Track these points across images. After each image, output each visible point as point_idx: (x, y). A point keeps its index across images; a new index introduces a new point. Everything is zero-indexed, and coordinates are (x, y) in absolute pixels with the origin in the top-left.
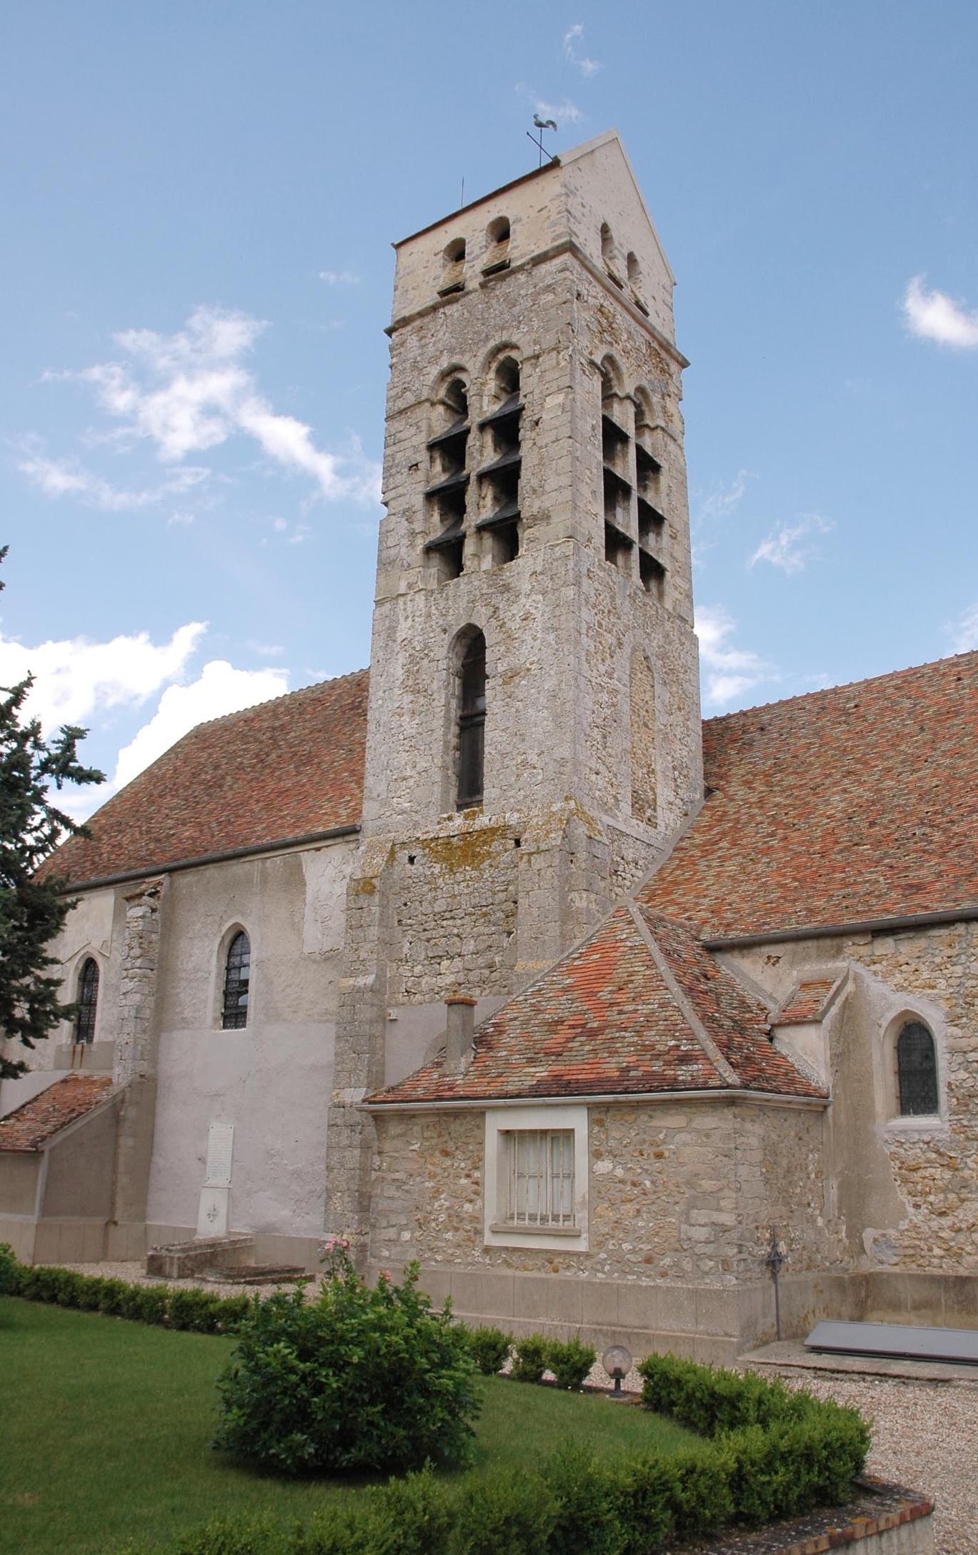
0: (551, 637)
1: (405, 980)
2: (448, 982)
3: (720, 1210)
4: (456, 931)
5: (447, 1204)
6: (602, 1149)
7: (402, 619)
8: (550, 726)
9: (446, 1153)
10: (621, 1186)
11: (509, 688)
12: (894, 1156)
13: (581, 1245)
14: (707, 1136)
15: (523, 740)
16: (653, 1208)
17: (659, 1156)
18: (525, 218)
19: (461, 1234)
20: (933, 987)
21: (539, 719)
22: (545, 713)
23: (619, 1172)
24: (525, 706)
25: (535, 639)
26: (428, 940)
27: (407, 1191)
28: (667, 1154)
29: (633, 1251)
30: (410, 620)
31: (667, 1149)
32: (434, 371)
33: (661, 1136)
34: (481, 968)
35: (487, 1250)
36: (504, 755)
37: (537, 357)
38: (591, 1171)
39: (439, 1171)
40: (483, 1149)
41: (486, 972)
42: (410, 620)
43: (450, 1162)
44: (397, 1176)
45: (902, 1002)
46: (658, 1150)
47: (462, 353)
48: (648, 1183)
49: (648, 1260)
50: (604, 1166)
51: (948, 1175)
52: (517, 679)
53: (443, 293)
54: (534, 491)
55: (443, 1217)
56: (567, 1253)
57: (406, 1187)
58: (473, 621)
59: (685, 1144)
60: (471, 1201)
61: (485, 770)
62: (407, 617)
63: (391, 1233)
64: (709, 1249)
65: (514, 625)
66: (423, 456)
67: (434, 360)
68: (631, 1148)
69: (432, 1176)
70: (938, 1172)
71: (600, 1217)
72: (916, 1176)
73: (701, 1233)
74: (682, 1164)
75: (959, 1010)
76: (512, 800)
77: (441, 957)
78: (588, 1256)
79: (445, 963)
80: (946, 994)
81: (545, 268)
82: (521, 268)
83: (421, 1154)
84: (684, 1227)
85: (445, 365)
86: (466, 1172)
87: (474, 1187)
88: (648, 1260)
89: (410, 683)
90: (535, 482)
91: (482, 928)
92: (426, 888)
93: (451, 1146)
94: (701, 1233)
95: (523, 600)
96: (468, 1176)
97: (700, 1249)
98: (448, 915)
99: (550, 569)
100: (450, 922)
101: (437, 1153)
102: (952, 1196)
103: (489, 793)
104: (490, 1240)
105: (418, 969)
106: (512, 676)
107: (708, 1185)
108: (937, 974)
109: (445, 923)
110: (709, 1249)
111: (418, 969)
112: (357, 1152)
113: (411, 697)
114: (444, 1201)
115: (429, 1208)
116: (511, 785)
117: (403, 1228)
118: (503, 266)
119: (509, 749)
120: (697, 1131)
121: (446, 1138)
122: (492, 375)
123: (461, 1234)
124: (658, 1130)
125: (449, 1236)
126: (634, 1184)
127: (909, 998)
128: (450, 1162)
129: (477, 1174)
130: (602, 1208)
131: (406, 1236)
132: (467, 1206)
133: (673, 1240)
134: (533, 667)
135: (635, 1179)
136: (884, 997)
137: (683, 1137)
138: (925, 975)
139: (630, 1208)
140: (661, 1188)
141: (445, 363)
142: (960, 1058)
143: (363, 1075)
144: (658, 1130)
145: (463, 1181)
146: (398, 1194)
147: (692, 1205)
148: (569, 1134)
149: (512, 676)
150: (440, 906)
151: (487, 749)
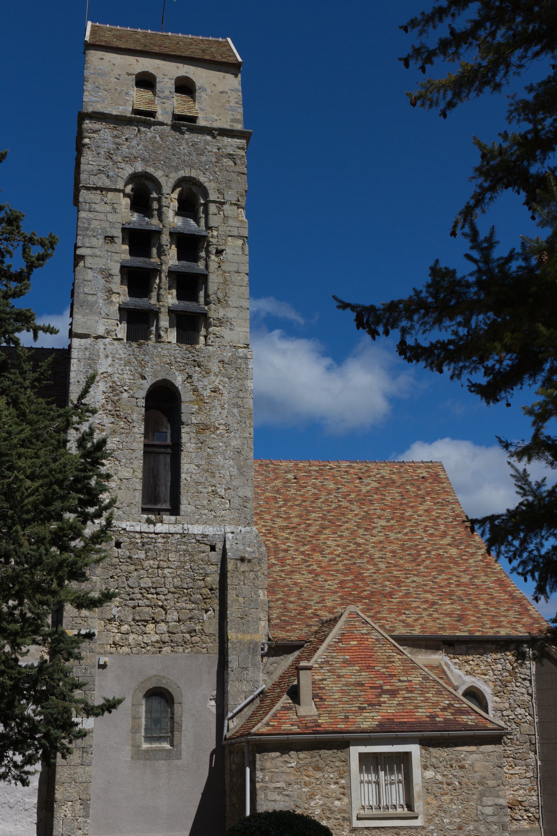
0: (235, 411)
1: (112, 634)
2: (154, 639)
3: (498, 797)
4: (160, 603)
5: (321, 802)
6: (428, 764)
7: (102, 356)
8: (235, 472)
9: (317, 768)
10: (441, 785)
11: (200, 436)
13: (418, 823)
14: (489, 756)
15: (214, 477)
16: (460, 797)
17: (462, 767)
18: (209, 91)
20: (486, 675)
21: (227, 466)
22: (231, 462)
23: (439, 777)
24: (215, 454)
25: (223, 408)
26: (134, 608)
27: (287, 795)
28: (467, 766)
29: (450, 823)
30: (110, 359)
31: (467, 763)
32: (129, 170)
33: (462, 756)
34: (182, 633)
35: (354, 830)
36: (198, 483)
37: (223, 204)
38: (423, 778)
39: (312, 780)
40: (348, 765)
41: (187, 636)
42: (110, 359)
43: (322, 774)
44: (278, 785)
45: (470, 681)
46: (460, 764)
47: (157, 168)
48: (457, 783)
49: (460, 828)
50: (430, 774)
52: (208, 432)
53: (136, 112)
54: (219, 301)
56: (410, 828)
57: (286, 793)
58: (169, 378)
59: (476, 761)
60: (339, 799)
61: (182, 491)
62: (107, 356)
64: (495, 819)
65: (207, 393)
66: (118, 233)
67: (129, 160)
68: (445, 763)
69: (306, 784)
71: (429, 804)
73: (489, 811)
74: (475, 772)
76: (204, 517)
77: (147, 621)
78: (423, 828)
79: (151, 626)
80: (493, 678)
81: (227, 140)
82: (208, 131)
83: (298, 769)
84: (480, 808)
85: (140, 170)
86: (335, 780)
87: (341, 790)
88: (460, 828)
89: (109, 407)
90: (220, 295)
91: (184, 604)
92: (132, 568)
93: (321, 763)
94: (489, 811)
95: (213, 378)
96: (336, 783)
97: (490, 819)
98: (153, 591)
99: (235, 363)
100: (155, 596)
101: (310, 769)
103: (184, 507)
104: (357, 824)
105: (125, 628)
106: (203, 428)
107: (491, 783)
108: (488, 668)
109: (150, 596)
110: (495, 819)
111: (125, 628)
113: (113, 420)
115: (306, 806)
116: (204, 506)
118: (193, 119)
119: (202, 480)
120: (482, 753)
121: (318, 758)
122: (175, 195)
124: (461, 752)
126: (448, 784)
127: (473, 679)
128: (322, 774)
129: (343, 781)
130: (430, 799)
132: (337, 803)
133: (473, 815)
134: (221, 427)
135: (449, 781)
136: (460, 677)
137: (475, 756)
138: (483, 667)
139: (447, 798)
140: (464, 786)
141: (139, 167)
142: (499, 714)
144: (461, 752)
145: (333, 786)
146: (278, 798)
147: (482, 795)
148: (407, 756)
149: (203, 428)
150: (146, 582)
151: (183, 476)
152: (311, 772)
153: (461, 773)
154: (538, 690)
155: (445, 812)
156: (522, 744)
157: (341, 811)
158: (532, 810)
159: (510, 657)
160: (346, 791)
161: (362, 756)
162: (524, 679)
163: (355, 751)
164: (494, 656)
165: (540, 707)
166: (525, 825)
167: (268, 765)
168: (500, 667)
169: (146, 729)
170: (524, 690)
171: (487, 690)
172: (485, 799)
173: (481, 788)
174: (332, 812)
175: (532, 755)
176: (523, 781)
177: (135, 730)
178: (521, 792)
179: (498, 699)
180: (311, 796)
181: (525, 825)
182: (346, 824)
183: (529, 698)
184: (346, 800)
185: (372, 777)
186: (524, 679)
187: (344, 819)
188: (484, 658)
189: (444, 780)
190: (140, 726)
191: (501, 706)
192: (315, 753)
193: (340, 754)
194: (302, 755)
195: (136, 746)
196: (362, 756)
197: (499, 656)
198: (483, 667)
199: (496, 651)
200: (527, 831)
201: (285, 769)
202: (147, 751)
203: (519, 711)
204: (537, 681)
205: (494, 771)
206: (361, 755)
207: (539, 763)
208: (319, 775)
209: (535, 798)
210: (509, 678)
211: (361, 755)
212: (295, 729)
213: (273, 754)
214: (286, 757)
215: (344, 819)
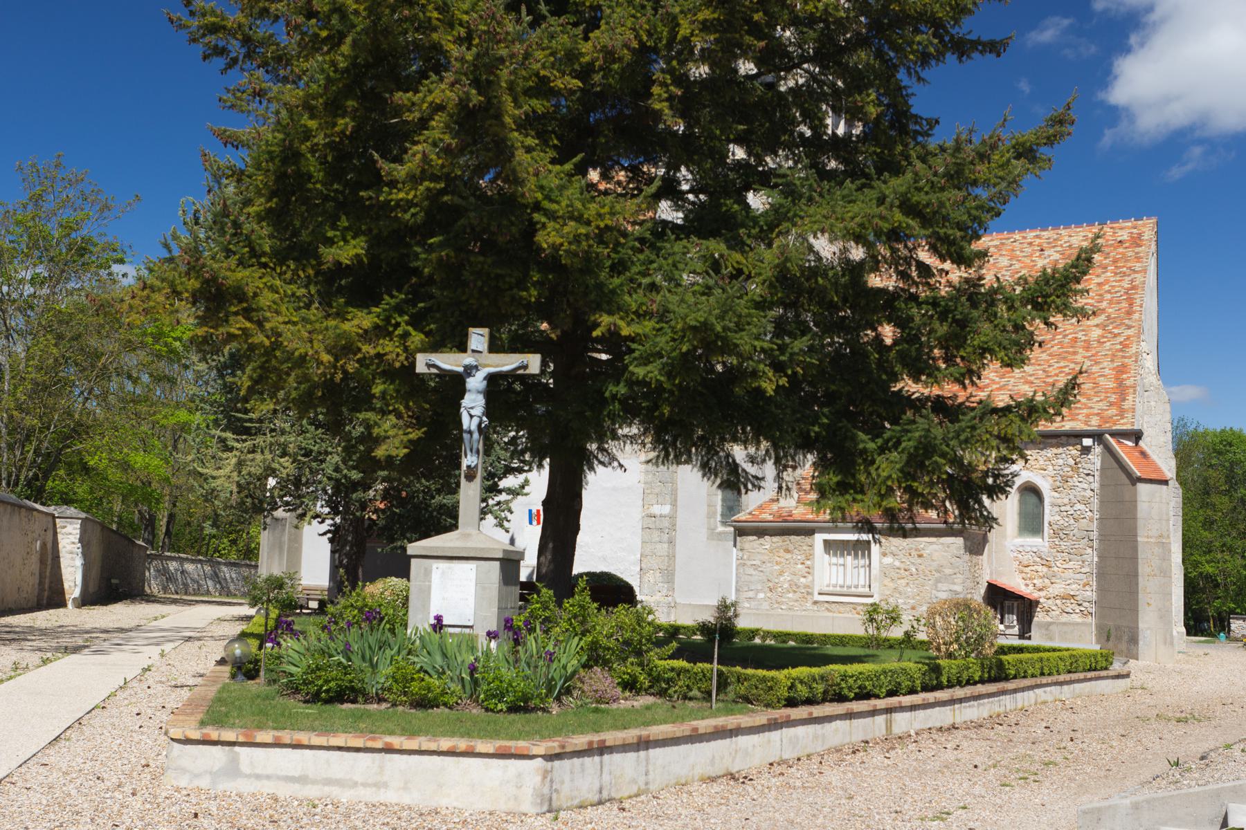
9: (787, 551)
12: (1016, 559)
17: (920, 556)
19: (798, 595)
23: (897, 563)
31: (925, 553)
35: (815, 603)
50: (888, 560)
51: (1045, 569)
55: (786, 586)
63: (751, 594)
69: (777, 563)
70: (1040, 568)
72: (1027, 570)
75: (1058, 484)
83: (771, 551)
93: (791, 547)
102: (1047, 581)
104: (818, 598)
107: (948, 571)
112: (666, 546)
114: (787, 577)
117: (758, 591)
123: (798, 595)
125: (790, 595)
129: (808, 563)
130: (887, 581)
131: (761, 595)
132: (802, 580)
138: (1042, 462)
142: (1057, 509)
143: (668, 497)
145: (800, 566)
147: (938, 581)
152: (782, 553)
153: (919, 561)
154: (1102, 486)
155: (900, 593)
156: (1078, 540)
157: (806, 586)
158: (1086, 604)
159: (1074, 452)
160: (810, 570)
161: (827, 543)
162: (1088, 475)
163: (819, 538)
164: (1055, 451)
165: (1102, 502)
166: (1076, 618)
167: (747, 546)
168: (1061, 462)
169: (722, 515)
170: (1086, 486)
171: (1044, 486)
172: (940, 585)
173: (937, 575)
174: (798, 587)
175: (1089, 551)
176: (1078, 576)
177: (711, 515)
178: (1074, 586)
179: (1056, 495)
180: (781, 573)
181: (1076, 618)
182: (809, 597)
183: (1091, 494)
184: (810, 578)
185: (841, 561)
186: (1088, 475)
187: (808, 593)
188: (1044, 452)
189: (902, 566)
190: (715, 513)
191: (1059, 502)
192: (786, 538)
193: (807, 540)
194: (775, 539)
195: (712, 530)
196: (827, 543)
197: (1060, 450)
198: (1042, 462)
199: (1058, 446)
200: (1078, 624)
201: (761, 550)
202: (720, 534)
203: (1078, 506)
204: (1101, 476)
205: (953, 560)
206: (826, 541)
207: (1096, 559)
208: (788, 556)
209: (1089, 593)
210: (1071, 473)
211: (826, 541)
212: (770, 518)
213: (751, 538)
214: (762, 540)
215: (808, 593)
